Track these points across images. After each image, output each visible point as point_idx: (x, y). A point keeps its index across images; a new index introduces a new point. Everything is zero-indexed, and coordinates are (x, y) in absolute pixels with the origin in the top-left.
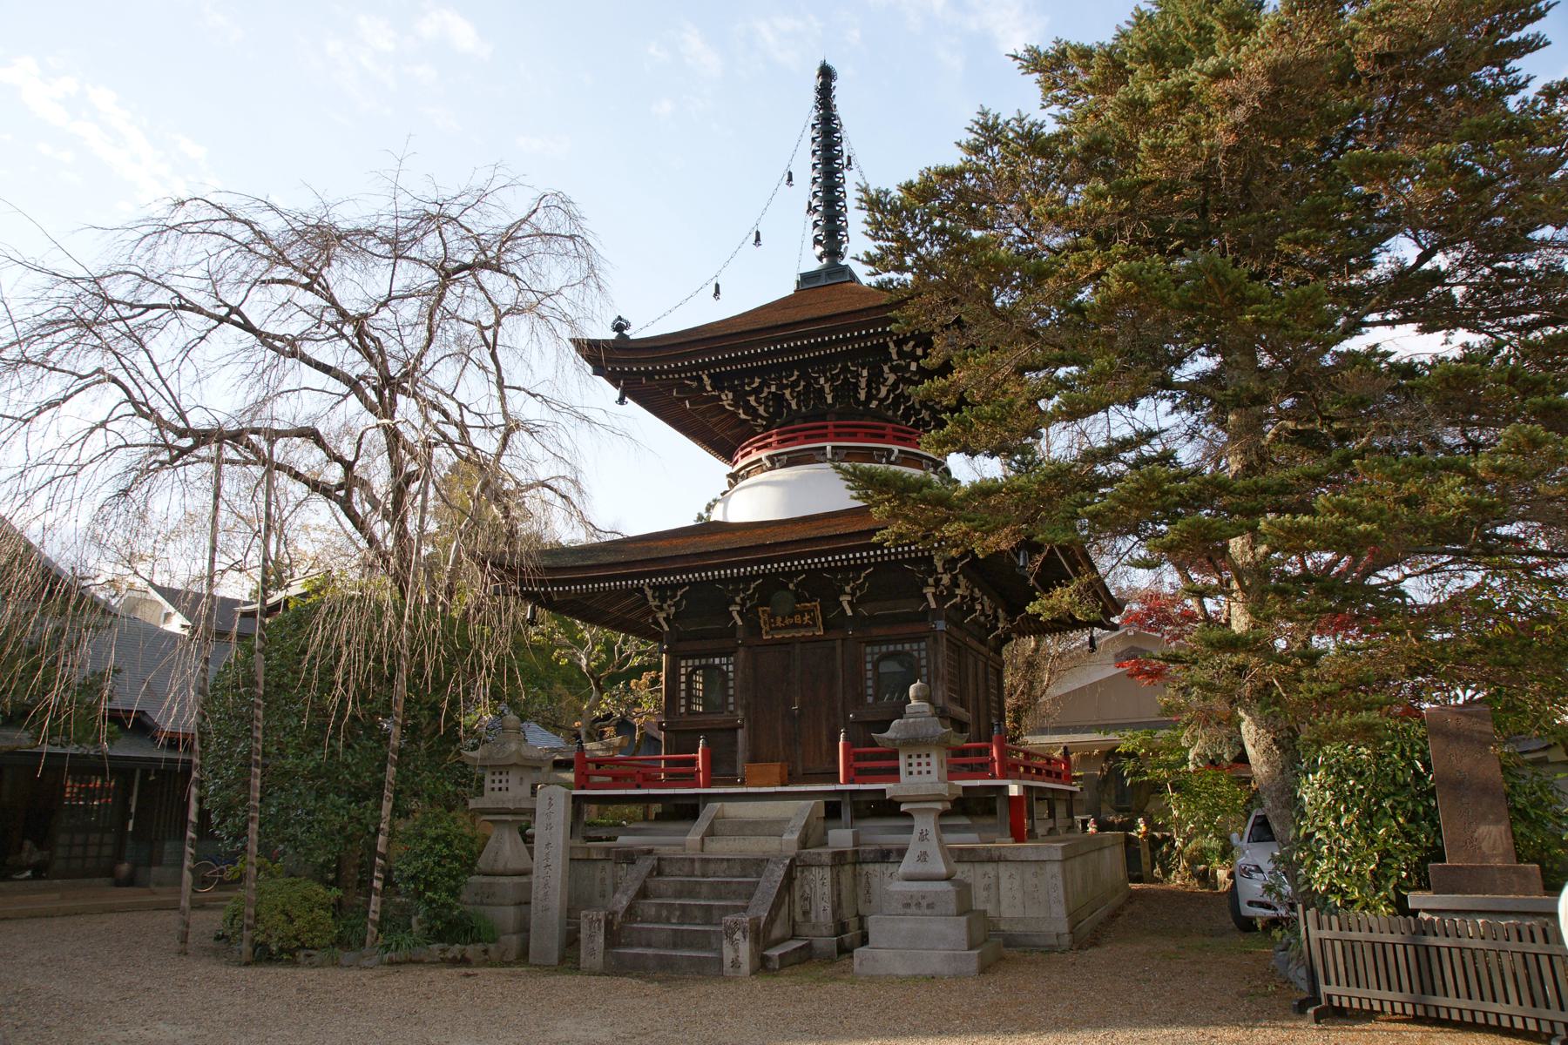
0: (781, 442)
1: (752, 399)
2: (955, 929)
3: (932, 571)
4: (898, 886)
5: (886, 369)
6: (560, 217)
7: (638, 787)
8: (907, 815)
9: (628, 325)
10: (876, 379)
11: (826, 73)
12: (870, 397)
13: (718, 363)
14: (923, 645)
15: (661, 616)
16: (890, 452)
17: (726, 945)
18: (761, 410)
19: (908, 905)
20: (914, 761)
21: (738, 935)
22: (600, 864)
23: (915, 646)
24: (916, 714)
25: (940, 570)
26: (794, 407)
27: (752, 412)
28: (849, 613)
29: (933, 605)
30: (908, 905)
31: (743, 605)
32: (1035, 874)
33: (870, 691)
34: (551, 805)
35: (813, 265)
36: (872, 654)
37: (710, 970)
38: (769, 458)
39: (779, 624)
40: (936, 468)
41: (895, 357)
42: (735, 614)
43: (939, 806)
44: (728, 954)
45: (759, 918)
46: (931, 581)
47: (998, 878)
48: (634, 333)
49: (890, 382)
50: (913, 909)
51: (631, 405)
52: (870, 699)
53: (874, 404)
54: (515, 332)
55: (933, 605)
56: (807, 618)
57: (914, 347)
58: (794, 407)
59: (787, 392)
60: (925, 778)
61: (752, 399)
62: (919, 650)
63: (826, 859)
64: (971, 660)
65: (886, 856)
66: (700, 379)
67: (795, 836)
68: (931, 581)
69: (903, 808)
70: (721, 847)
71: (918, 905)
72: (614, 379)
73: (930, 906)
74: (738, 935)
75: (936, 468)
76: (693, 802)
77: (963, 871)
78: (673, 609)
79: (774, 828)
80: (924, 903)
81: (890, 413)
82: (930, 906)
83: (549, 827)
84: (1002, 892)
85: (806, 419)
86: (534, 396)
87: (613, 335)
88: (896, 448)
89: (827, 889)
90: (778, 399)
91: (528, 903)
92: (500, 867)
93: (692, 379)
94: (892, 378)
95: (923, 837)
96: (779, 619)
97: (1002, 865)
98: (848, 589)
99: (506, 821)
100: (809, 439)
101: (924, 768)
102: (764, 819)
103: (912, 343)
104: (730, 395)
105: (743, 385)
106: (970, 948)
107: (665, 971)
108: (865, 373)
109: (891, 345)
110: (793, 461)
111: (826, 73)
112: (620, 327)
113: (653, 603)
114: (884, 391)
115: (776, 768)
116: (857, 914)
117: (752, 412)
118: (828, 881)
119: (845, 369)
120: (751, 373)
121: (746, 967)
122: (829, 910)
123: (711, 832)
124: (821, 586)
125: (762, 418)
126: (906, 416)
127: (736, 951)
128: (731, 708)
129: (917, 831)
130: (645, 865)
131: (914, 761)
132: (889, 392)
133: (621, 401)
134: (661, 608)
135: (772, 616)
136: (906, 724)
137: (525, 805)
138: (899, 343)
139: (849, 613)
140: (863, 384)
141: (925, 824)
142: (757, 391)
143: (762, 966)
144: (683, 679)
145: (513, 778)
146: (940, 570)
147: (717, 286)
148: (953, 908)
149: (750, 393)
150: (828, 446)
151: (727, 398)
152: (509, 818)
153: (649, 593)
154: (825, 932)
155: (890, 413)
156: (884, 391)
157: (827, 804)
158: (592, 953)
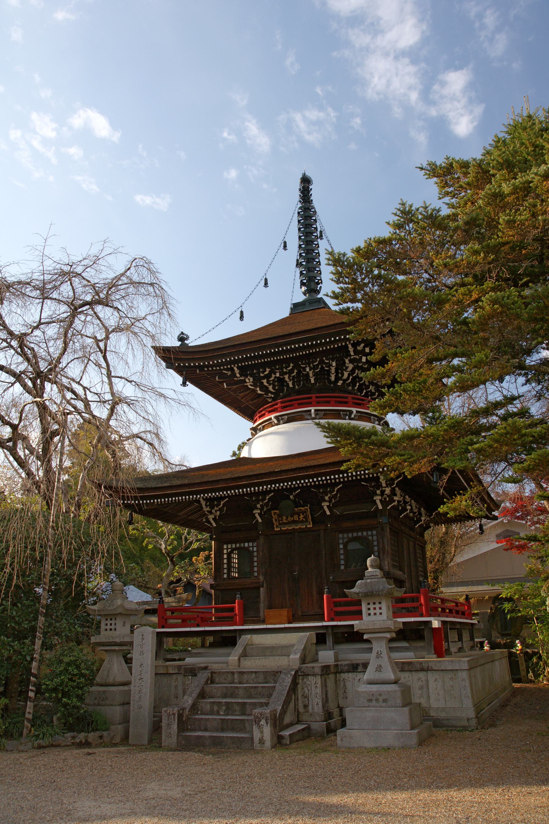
0: (284, 408)
1: (265, 381)
2: (401, 717)
3: (379, 486)
4: (363, 688)
5: (347, 361)
6: (145, 272)
7: (198, 626)
8: (368, 641)
9: (187, 338)
10: (341, 367)
11: (306, 181)
12: (337, 379)
13: (243, 360)
14: (374, 532)
15: (211, 517)
16: (351, 412)
18: (271, 388)
19: (370, 700)
20: (372, 606)
21: (263, 722)
22: (175, 677)
23: (370, 533)
24: (372, 577)
25: (384, 485)
26: (291, 385)
27: (264, 388)
28: (328, 513)
29: (380, 507)
30: (370, 700)
31: (262, 509)
32: (451, 679)
33: (342, 562)
34: (143, 639)
35: (300, 297)
36: (343, 538)
37: (245, 745)
38: (276, 417)
39: (285, 521)
40: (379, 421)
41: (352, 353)
42: (257, 515)
43: (388, 635)
45: (276, 710)
46: (378, 492)
47: (427, 681)
48: (192, 342)
49: (350, 369)
50: (374, 703)
51: (191, 387)
52: (342, 567)
53: (340, 383)
54: (119, 342)
55: (380, 507)
56: (302, 516)
57: (364, 347)
58: (291, 385)
59: (286, 377)
60: (378, 617)
61: (265, 381)
62: (372, 535)
63: (318, 670)
64: (405, 540)
65: (354, 668)
66: (232, 370)
67: (298, 656)
68: (378, 492)
69: (365, 637)
70: (250, 664)
71: (377, 700)
72: (179, 370)
73: (385, 701)
74: (263, 722)
75: (379, 421)
76: (234, 635)
77: (405, 677)
78: (218, 513)
79: (284, 651)
80: (381, 699)
81: (350, 388)
82: (385, 701)
83: (142, 653)
84: (431, 691)
85: (298, 392)
86: (131, 382)
87: (178, 344)
88: (354, 410)
89: (319, 690)
90: (281, 381)
91: (129, 703)
92: (110, 680)
93: (227, 370)
94: (351, 366)
95: (379, 655)
96: (284, 518)
97: (429, 673)
98: (327, 498)
99: (115, 650)
100: (301, 405)
101: (378, 611)
102: (278, 644)
103: (362, 345)
104: (251, 380)
105: (259, 373)
106: (412, 729)
107: (217, 747)
108: (334, 364)
109: (350, 346)
110: (291, 419)
111: (306, 181)
112: (182, 338)
113: (206, 509)
114: (346, 375)
115: (284, 612)
116: (339, 707)
117: (264, 388)
118: (319, 685)
119: (322, 362)
120: (264, 365)
121: (268, 744)
122: (320, 704)
123: (244, 654)
124: (310, 497)
125: (272, 393)
126: (360, 390)
127: (262, 732)
128: (256, 574)
129: (374, 651)
130: (203, 676)
131: (372, 606)
132: (349, 375)
133: (184, 384)
134: (211, 512)
135: (280, 516)
136: (366, 584)
137: (127, 639)
138: (355, 345)
139: (328, 513)
140: (333, 370)
141: (380, 647)
142: (268, 377)
143: (279, 742)
144: (225, 556)
145: (119, 622)
146: (384, 485)
147: (242, 313)
148: (399, 701)
149: (264, 378)
150: (313, 409)
151: (249, 381)
152: (116, 648)
153: (203, 503)
154: (318, 719)
155: (350, 388)
156: (346, 375)
157: (317, 634)
158: (169, 736)
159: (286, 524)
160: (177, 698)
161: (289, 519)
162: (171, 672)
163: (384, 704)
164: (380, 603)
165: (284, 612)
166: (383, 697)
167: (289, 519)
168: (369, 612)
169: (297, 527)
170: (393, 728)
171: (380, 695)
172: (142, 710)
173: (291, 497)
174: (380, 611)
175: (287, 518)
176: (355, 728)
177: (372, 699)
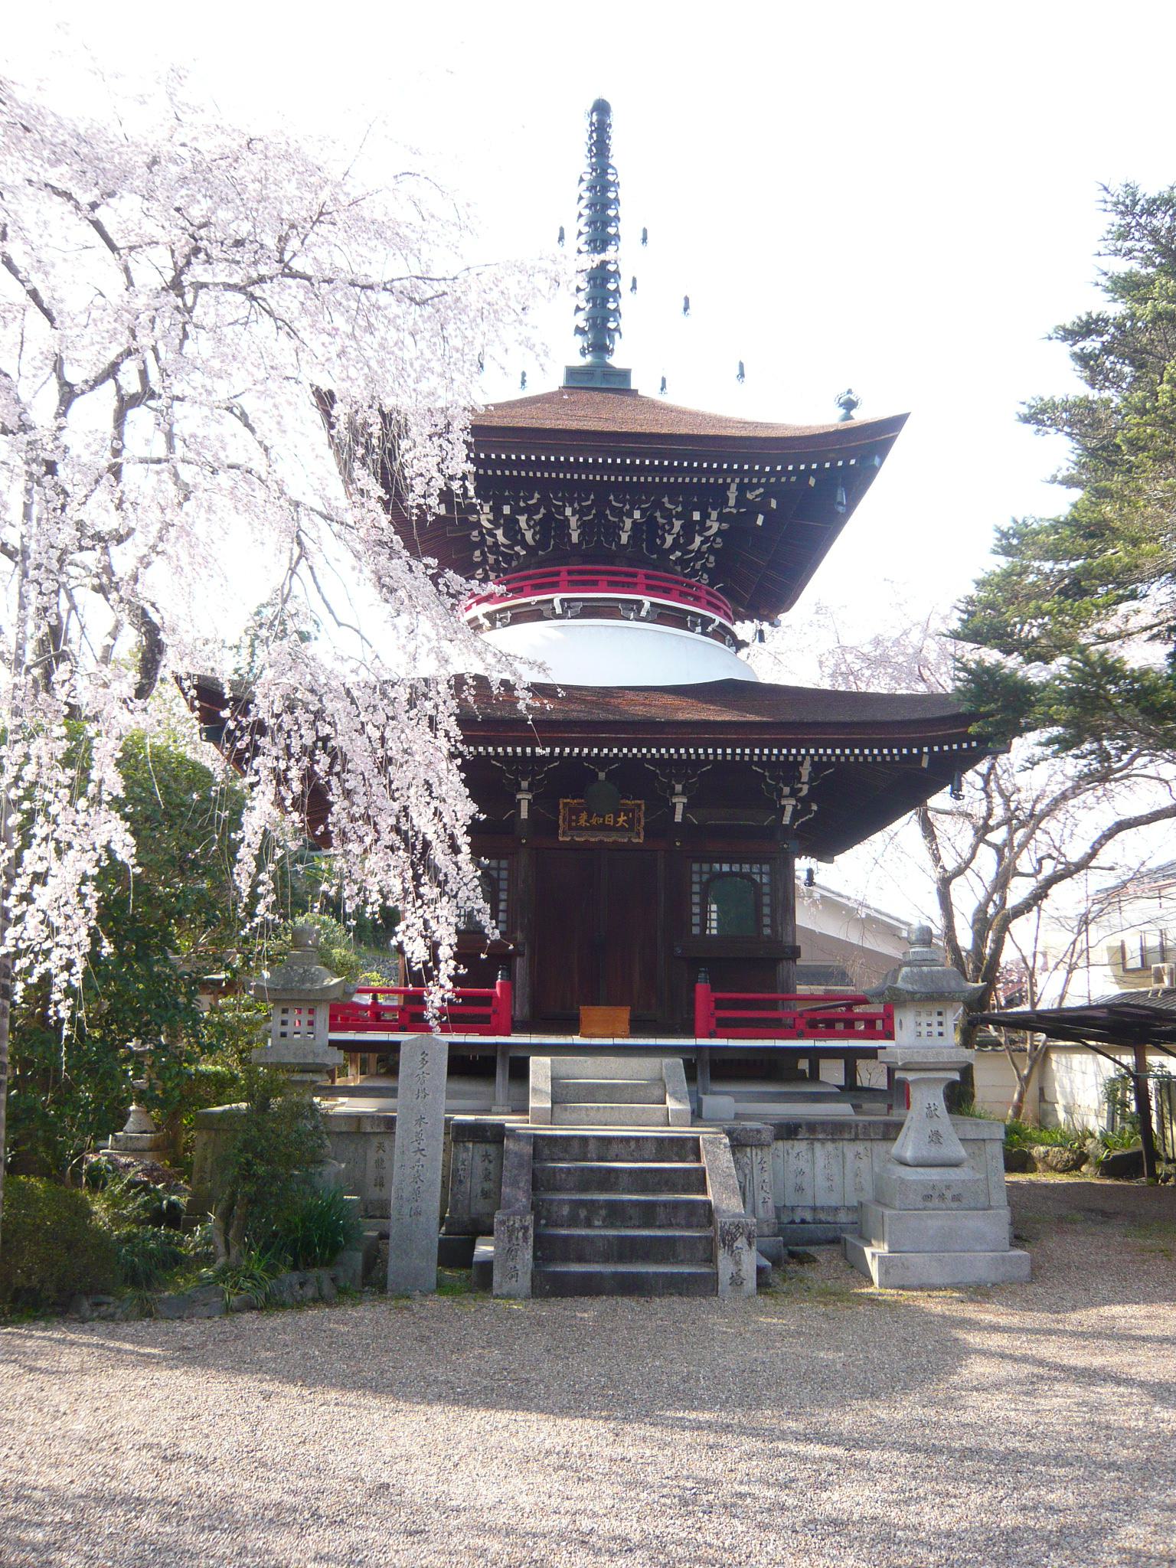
12: (676, 545)
14: (766, 868)
17: (722, 1255)
19: (928, 1197)
21: (741, 1242)
30: (928, 1197)
34: (424, 1062)
36: (701, 873)
39: (582, 822)
41: (732, 502)
44: (725, 1265)
46: (787, 790)
50: (936, 1202)
68: (787, 790)
71: (942, 1197)
73: (956, 1198)
76: (487, 1053)
80: (949, 1194)
82: (956, 1198)
85: (586, 558)
96: (584, 816)
109: (733, 487)
110: (591, 611)
115: (624, 1014)
127: (738, 1263)
135: (575, 811)
138: (742, 489)
150: (647, 601)
159: (586, 829)
160: (382, 1185)
161: (594, 821)
162: (369, 1130)
163: (954, 1205)
164: (940, 1014)
165: (624, 1014)
166: (955, 1191)
167: (594, 821)
168: (919, 1029)
169: (610, 840)
170: (978, 1248)
171: (948, 1187)
172: (422, 1219)
173: (602, 775)
174: (940, 1029)
175: (590, 817)
176: (904, 1248)
177: (931, 1196)
